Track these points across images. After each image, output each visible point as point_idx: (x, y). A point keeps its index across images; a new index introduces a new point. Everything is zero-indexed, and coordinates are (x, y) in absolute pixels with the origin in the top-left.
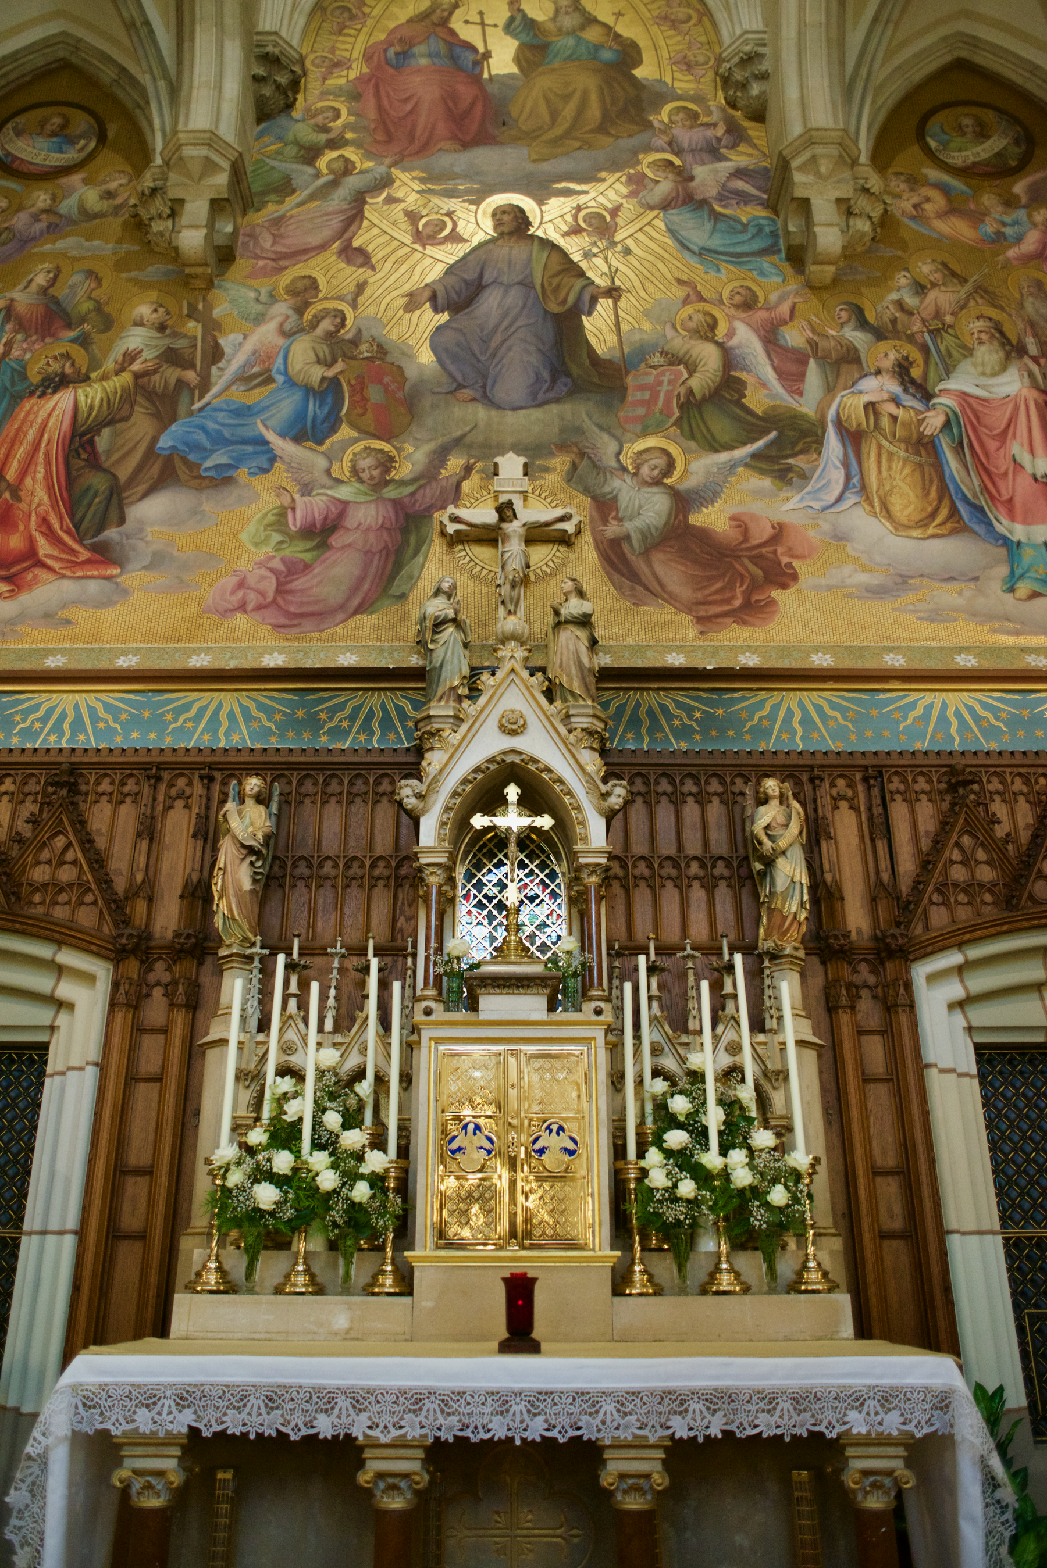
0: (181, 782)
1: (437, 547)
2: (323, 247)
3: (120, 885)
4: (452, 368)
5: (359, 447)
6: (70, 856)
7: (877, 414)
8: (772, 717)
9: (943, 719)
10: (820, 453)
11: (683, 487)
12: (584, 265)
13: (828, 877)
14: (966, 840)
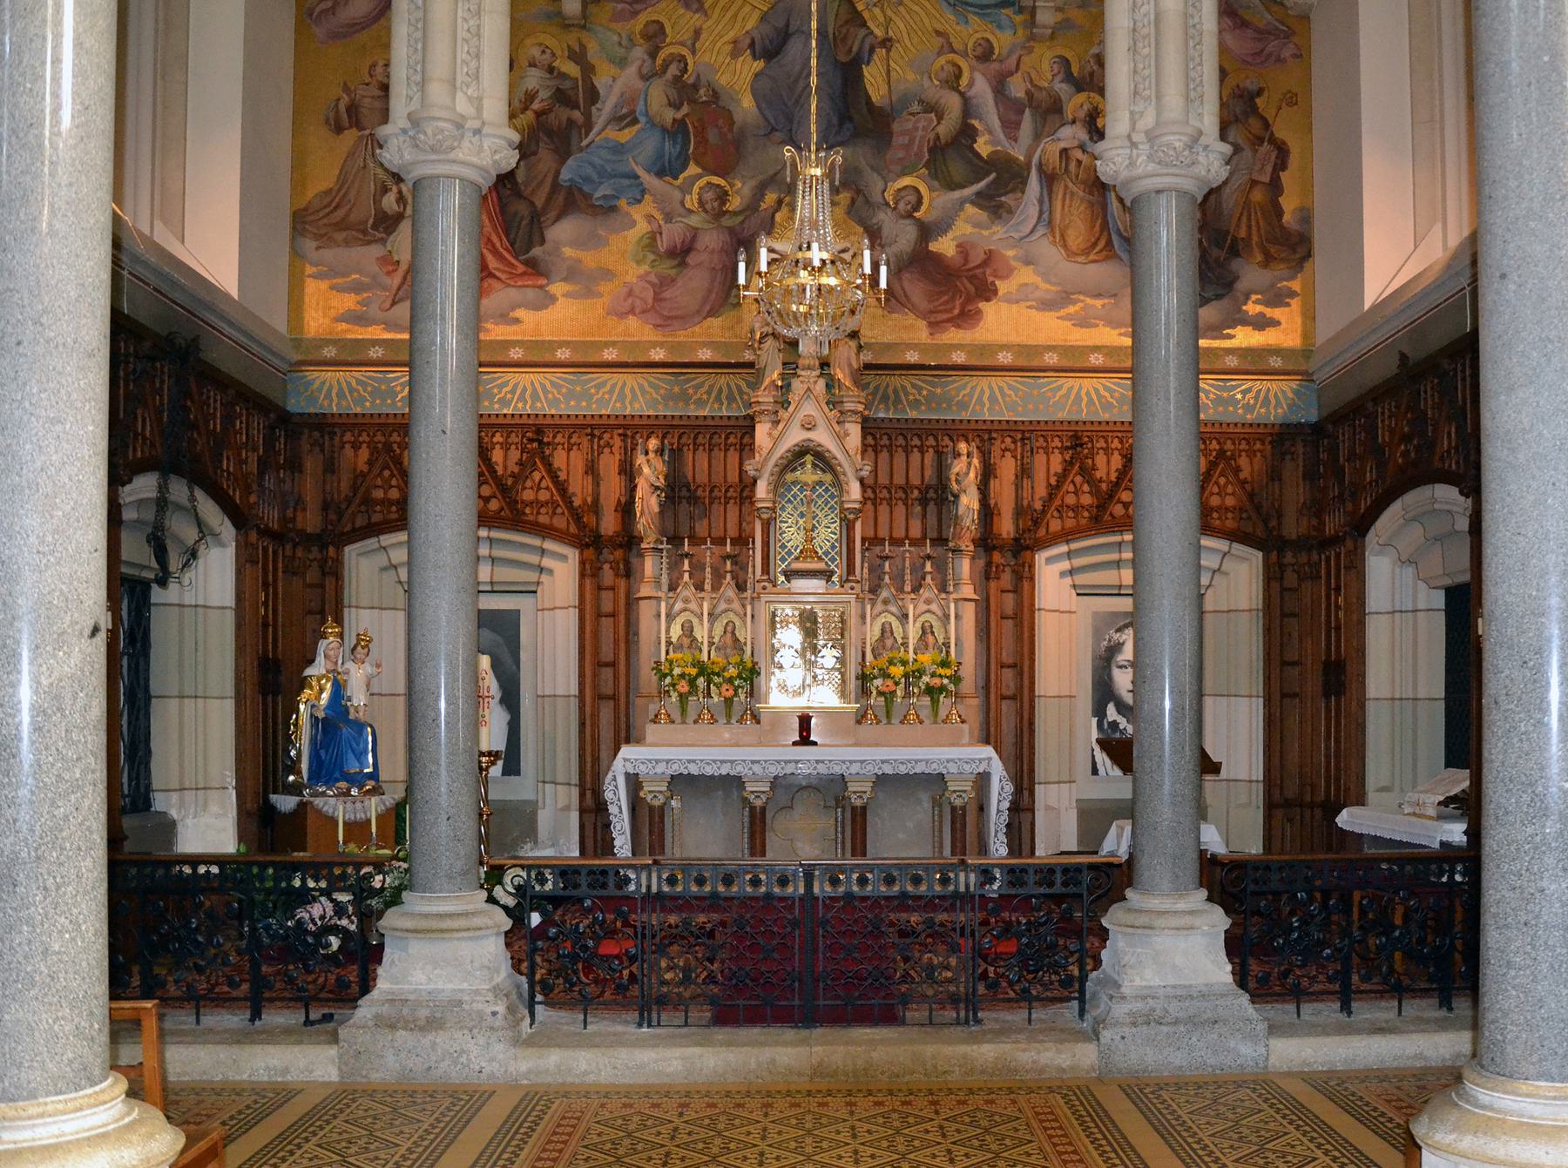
0: (606, 436)
3: (577, 502)
4: (767, 113)
6: (543, 484)
7: (1068, 158)
8: (971, 395)
9: (1078, 398)
10: (1023, 192)
11: (926, 220)
12: (866, 15)
13: (992, 502)
14: (1079, 479)
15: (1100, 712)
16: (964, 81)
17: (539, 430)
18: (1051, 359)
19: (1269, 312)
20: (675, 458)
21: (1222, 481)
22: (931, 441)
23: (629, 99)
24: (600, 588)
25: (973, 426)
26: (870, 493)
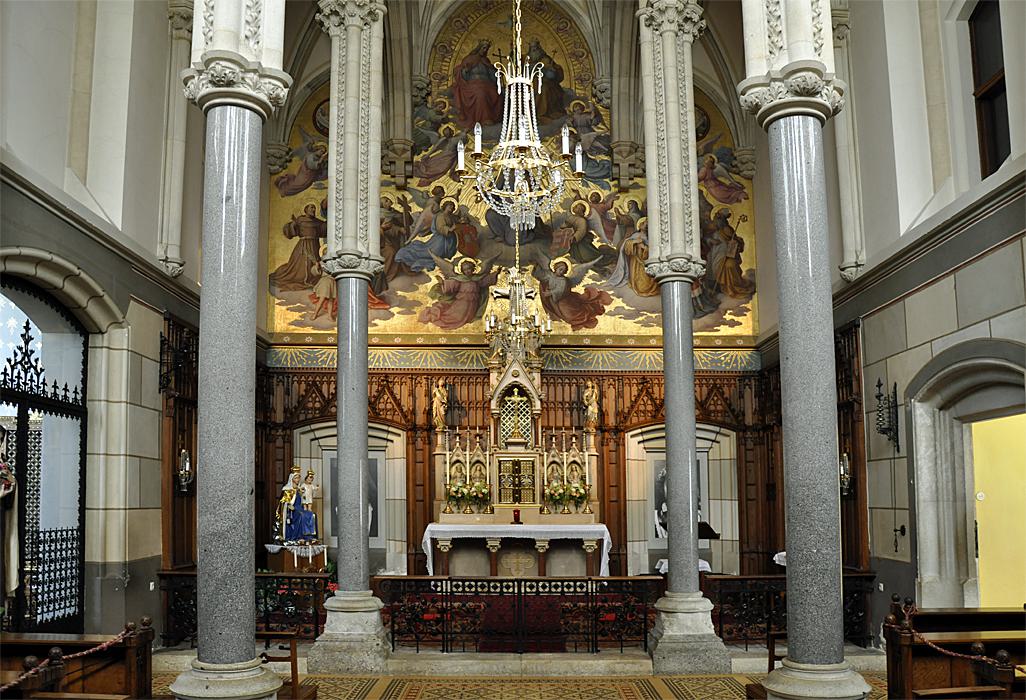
1: (491, 299)
2: (444, 173)
3: (405, 409)
5: (463, 260)
8: (593, 359)
9: (645, 360)
14: (645, 398)
15: (658, 508)
16: (587, 213)
17: (387, 376)
18: (631, 342)
19: (736, 319)
20: (451, 389)
21: (715, 398)
22: (574, 381)
23: (427, 222)
24: (416, 450)
25: (595, 374)
26: (545, 405)
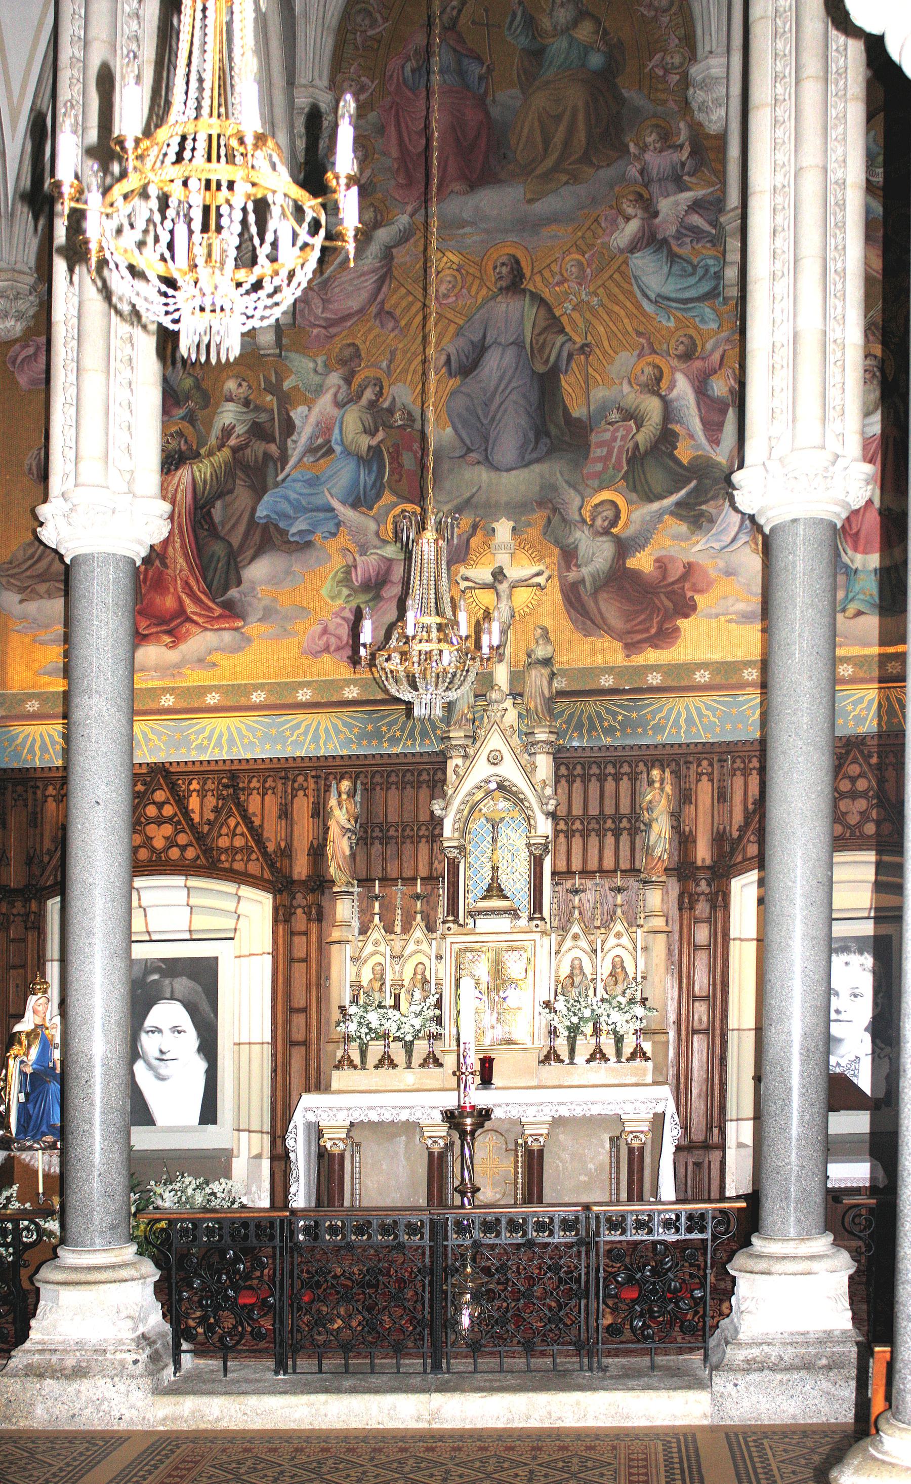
3: (271, 847)
5: (397, 510)
11: (623, 536)
16: (664, 384)
